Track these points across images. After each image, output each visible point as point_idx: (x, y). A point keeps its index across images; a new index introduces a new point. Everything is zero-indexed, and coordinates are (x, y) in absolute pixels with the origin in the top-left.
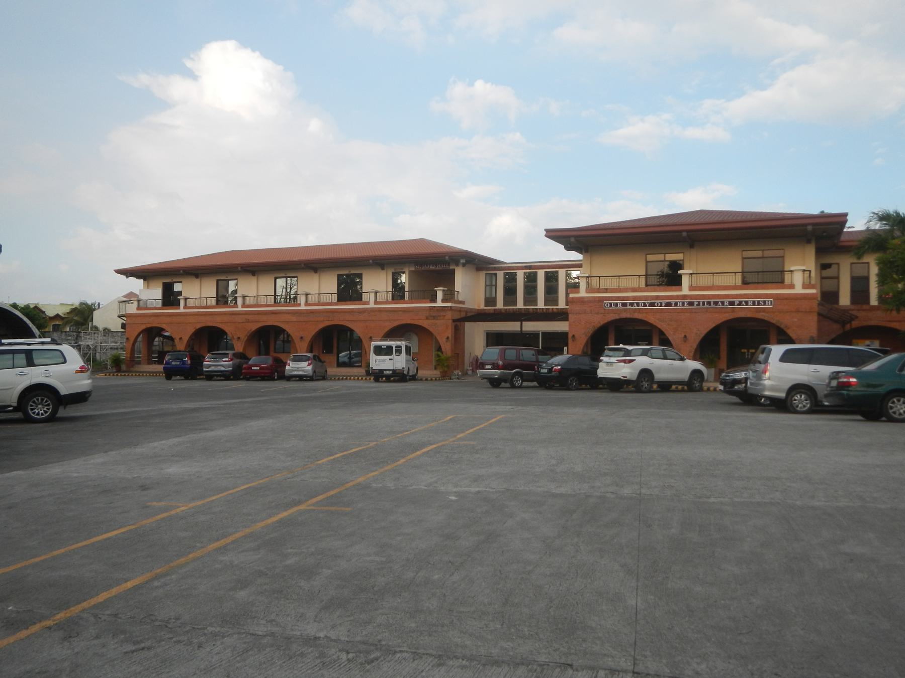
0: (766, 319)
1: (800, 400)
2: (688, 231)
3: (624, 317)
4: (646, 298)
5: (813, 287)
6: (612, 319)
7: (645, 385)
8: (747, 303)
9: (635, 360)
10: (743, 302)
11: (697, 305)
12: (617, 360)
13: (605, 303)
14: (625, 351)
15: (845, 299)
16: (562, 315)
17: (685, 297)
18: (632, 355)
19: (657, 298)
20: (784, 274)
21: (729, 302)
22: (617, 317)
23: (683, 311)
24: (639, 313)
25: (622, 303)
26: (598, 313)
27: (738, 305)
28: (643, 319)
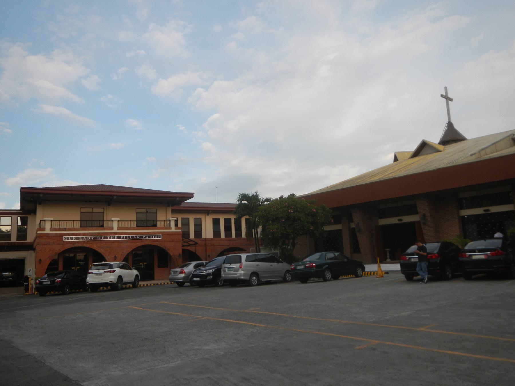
0: (158, 245)
1: (254, 280)
2: (117, 196)
3: (77, 246)
4: (92, 234)
5: (179, 228)
6: (69, 247)
7: (120, 285)
8: (149, 237)
9: (115, 271)
10: (85, 238)
11: (122, 238)
12: (105, 271)
13: (64, 238)
14: (109, 265)
15: (192, 236)
16: (30, 247)
17: (115, 234)
18: (114, 267)
19: (99, 234)
20: (157, 222)
21: (140, 236)
22: (72, 246)
23: (114, 242)
24: (87, 243)
25: (76, 237)
26: (59, 244)
27: (144, 238)
28: (90, 247)
